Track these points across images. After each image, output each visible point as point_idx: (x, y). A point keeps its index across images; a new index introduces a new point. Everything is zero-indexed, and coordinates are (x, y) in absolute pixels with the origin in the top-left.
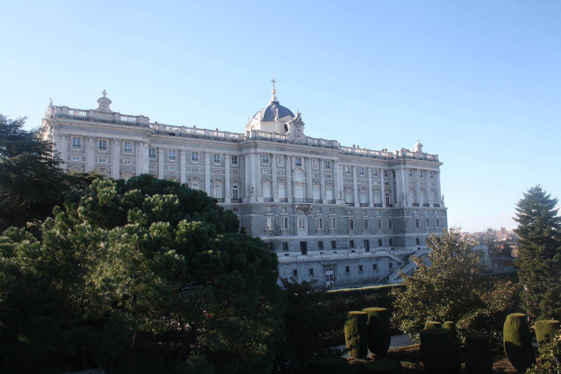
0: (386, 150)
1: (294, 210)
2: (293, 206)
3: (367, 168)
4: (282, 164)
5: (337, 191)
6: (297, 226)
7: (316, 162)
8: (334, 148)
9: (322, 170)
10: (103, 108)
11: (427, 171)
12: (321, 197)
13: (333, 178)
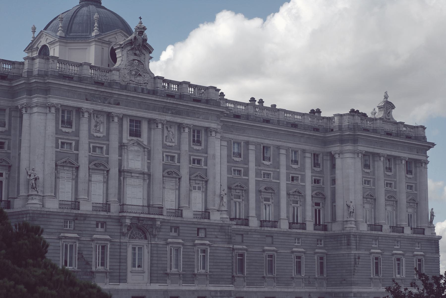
0: (319, 111)
2: (120, 220)
3: (279, 148)
4: (101, 130)
5: (214, 193)
6: (126, 262)
7: (173, 130)
9: (185, 147)
11: (401, 160)
12: (179, 204)
13: (206, 164)
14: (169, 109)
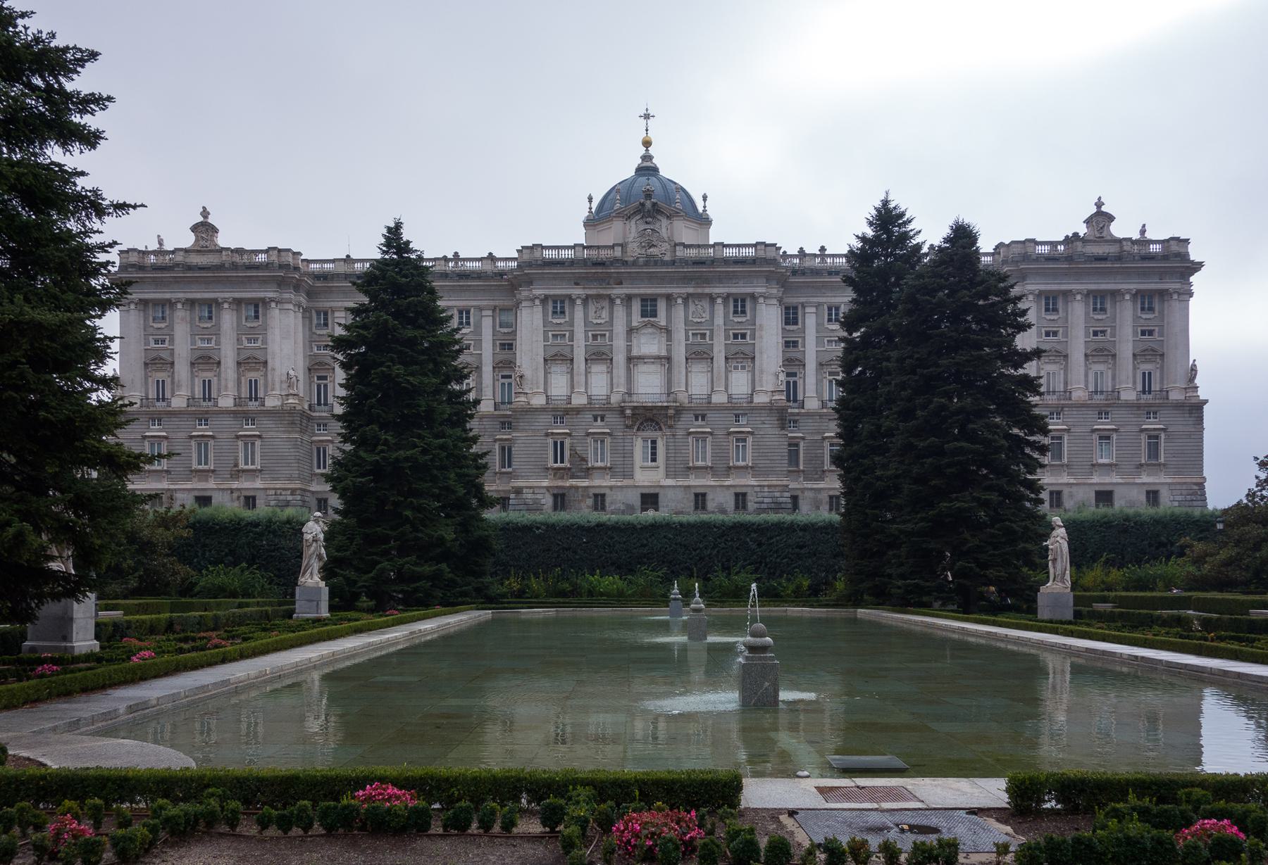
2: (622, 410)
4: (604, 316)
9: (719, 320)
10: (202, 243)
12: (712, 389)
14: (692, 280)
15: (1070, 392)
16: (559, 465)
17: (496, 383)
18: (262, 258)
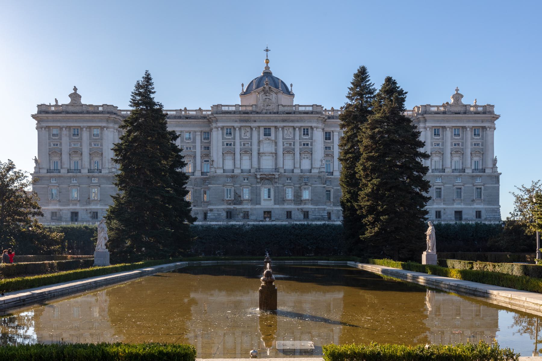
1: (257, 180)
4: (248, 135)
8: (313, 113)
9: (297, 137)
12: (294, 166)
13: (312, 145)
15: (444, 169)
16: (229, 199)
17: (202, 163)
18: (101, 109)
